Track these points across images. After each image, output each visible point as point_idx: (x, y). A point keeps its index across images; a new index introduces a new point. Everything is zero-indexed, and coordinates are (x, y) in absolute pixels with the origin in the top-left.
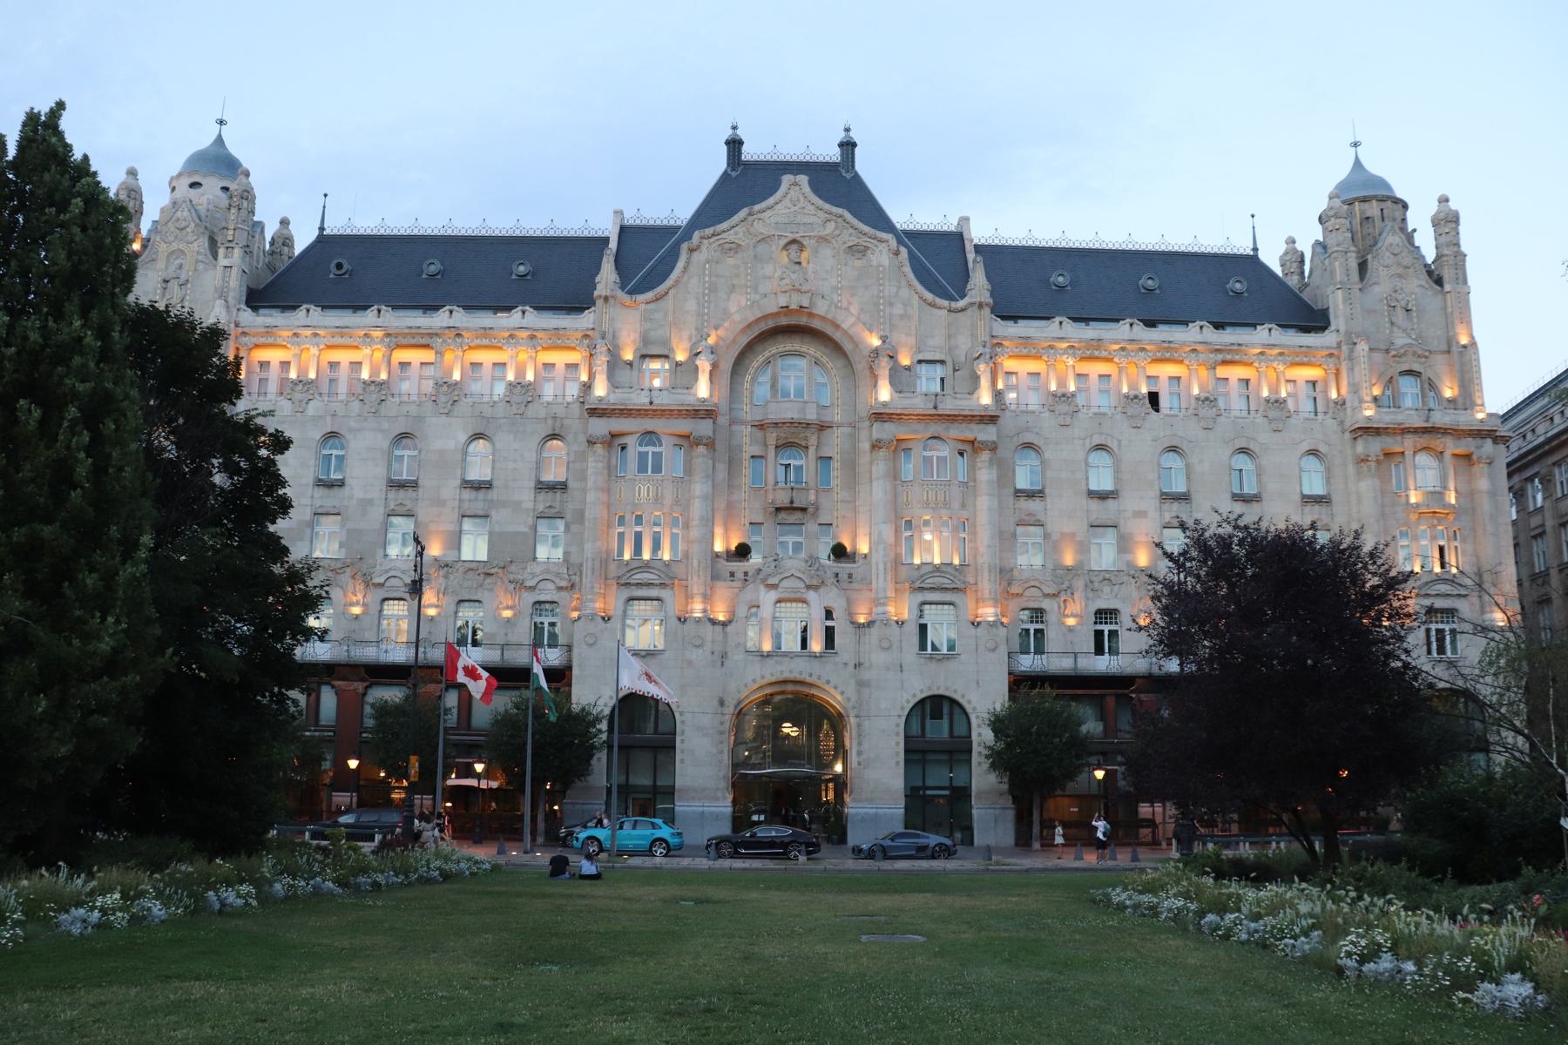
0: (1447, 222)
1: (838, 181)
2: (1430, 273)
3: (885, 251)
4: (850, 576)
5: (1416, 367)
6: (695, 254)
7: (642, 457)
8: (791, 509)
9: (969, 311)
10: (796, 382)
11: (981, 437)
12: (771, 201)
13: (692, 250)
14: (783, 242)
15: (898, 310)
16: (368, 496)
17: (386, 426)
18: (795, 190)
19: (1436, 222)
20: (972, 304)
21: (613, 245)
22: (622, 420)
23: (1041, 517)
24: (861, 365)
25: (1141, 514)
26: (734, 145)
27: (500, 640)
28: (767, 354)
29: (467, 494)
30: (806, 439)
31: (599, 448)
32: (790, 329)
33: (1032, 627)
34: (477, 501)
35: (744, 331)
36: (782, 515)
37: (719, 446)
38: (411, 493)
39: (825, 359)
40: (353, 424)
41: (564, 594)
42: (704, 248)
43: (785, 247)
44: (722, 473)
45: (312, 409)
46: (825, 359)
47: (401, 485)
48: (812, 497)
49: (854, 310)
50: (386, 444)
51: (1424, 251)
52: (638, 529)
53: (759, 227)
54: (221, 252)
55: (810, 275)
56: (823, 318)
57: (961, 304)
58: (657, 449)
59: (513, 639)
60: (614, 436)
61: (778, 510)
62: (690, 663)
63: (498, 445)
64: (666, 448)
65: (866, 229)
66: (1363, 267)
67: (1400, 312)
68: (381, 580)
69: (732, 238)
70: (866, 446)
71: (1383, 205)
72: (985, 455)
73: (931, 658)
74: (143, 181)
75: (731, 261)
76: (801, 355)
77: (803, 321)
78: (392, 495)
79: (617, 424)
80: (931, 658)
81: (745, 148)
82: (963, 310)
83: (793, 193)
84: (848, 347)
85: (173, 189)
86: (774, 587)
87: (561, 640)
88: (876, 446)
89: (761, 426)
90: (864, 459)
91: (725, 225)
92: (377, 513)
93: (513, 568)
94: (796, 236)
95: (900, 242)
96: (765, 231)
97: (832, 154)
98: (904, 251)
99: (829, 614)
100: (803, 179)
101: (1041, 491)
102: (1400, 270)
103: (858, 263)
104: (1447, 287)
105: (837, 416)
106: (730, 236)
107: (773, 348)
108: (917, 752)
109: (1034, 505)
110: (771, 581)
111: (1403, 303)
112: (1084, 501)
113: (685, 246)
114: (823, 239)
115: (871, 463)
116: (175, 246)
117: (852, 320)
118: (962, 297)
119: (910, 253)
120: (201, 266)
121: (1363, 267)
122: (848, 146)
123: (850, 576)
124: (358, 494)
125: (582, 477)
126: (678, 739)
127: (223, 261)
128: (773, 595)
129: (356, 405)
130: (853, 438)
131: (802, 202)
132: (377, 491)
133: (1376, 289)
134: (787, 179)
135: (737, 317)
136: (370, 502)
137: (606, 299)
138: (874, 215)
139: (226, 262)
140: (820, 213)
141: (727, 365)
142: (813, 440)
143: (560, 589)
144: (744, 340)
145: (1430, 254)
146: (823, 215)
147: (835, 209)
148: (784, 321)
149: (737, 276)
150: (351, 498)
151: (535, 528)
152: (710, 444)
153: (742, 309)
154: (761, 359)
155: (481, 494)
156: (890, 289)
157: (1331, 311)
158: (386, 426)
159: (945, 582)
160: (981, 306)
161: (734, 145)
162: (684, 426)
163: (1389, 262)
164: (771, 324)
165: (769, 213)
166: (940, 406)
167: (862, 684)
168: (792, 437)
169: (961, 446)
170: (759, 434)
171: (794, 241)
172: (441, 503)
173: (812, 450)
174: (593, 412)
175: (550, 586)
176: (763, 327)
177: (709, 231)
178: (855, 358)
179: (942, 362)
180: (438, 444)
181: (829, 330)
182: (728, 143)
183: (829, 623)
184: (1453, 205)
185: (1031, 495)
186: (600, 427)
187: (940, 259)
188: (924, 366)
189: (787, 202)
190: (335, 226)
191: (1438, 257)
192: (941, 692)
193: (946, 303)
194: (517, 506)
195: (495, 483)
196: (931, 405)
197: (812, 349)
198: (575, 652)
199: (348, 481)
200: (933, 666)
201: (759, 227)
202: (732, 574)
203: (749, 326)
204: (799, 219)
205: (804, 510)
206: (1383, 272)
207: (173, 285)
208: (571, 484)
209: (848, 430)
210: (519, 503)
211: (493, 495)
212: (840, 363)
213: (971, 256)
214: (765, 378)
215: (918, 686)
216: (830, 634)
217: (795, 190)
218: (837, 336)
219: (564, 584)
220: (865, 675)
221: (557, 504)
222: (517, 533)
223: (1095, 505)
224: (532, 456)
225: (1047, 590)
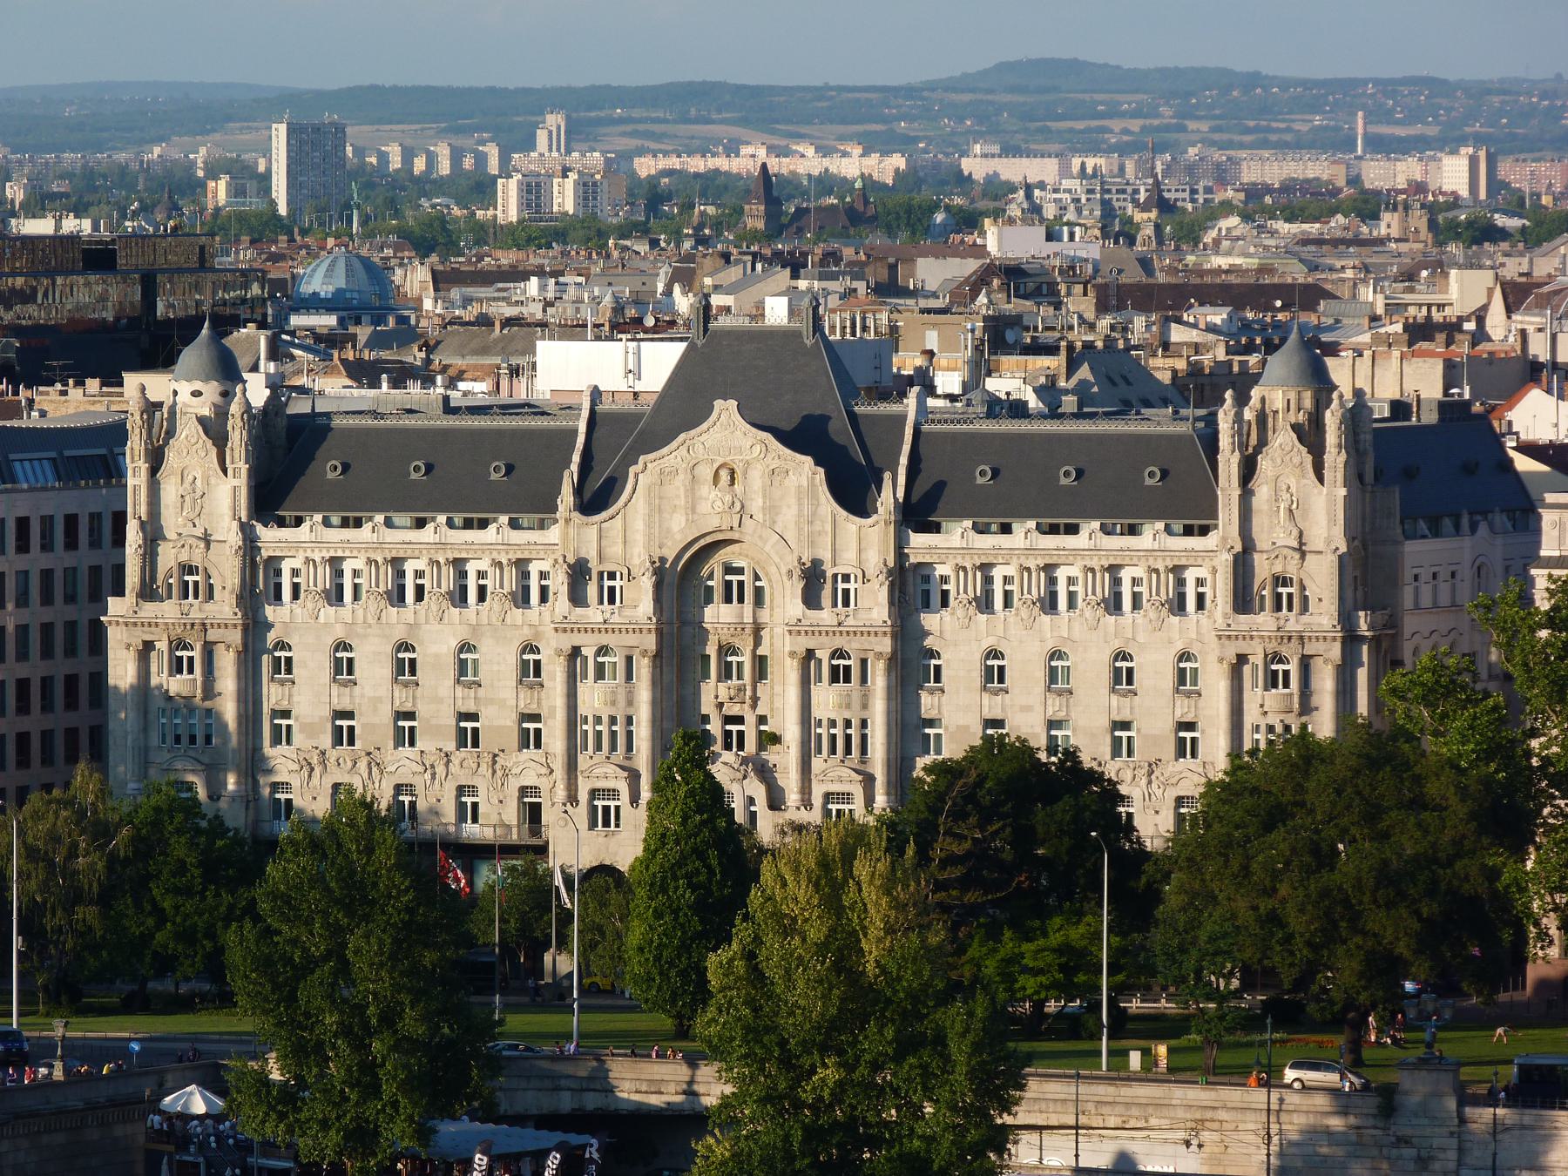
12: (705, 426)
14: (716, 466)
18: (726, 410)
25: (1027, 709)
41: (544, 779)
54: (230, 472)
91: (665, 450)
94: (728, 459)
98: (821, 470)
113: (632, 470)
134: (718, 403)
135: (678, 537)
136: (380, 699)
139: (236, 482)
149: (678, 496)
150: (362, 696)
162: (631, 640)
172: (440, 701)
180: (434, 649)
211: (481, 692)
217: (726, 410)
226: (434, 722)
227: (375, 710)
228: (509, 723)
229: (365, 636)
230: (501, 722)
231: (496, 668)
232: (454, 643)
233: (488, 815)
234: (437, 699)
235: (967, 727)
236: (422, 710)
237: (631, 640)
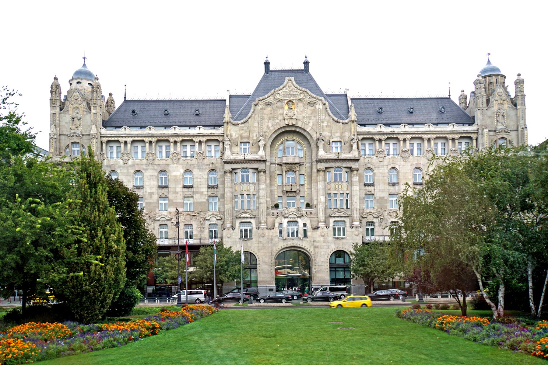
0: (519, 83)
1: (303, 74)
2: (512, 102)
3: (321, 103)
4: (311, 213)
5: (505, 136)
6: (257, 106)
8: (291, 192)
9: (349, 124)
10: (293, 151)
11: (353, 167)
13: (256, 105)
14: (286, 101)
15: (325, 124)
16: (152, 191)
17: (156, 167)
19: (516, 83)
20: (350, 121)
21: (227, 103)
22: (235, 164)
23: (373, 192)
24: (313, 144)
27: (199, 236)
28: (282, 140)
29: (186, 190)
30: (295, 168)
31: (228, 174)
32: (290, 131)
33: (370, 228)
34: (188, 192)
35: (274, 133)
36: (289, 194)
37: (267, 172)
38: (166, 190)
39: (301, 141)
40: (144, 167)
41: (219, 221)
42: (259, 104)
43: (287, 103)
44: (268, 181)
45: (130, 162)
46: (301, 141)
47: (163, 187)
48: (298, 188)
49: (311, 125)
50: (156, 174)
51: (510, 94)
52: (242, 200)
54: (92, 108)
55: (296, 113)
56: (300, 128)
58: (247, 174)
59: (203, 236)
60: (233, 169)
61: (287, 192)
62: (261, 242)
63: (194, 173)
64: (251, 173)
65: (314, 96)
66: (488, 101)
67: (501, 117)
68: (158, 219)
69: (269, 100)
70: (315, 171)
71: (497, 77)
72: (355, 172)
73: (337, 238)
74: (60, 81)
75: (269, 109)
76: (293, 140)
77: (293, 129)
78: (160, 191)
80: (337, 238)
81: (270, 65)
82: (347, 123)
83: (290, 84)
84: (308, 137)
85: (71, 84)
86: (287, 217)
87: (219, 236)
88: (318, 171)
89: (281, 165)
90: (315, 175)
91: (266, 96)
92: (156, 197)
93: (202, 213)
94: (291, 99)
95: (326, 100)
96: (280, 98)
98: (327, 103)
99: (305, 225)
100: (292, 78)
101: (373, 184)
102: (501, 102)
103: (312, 108)
104: (518, 107)
105: (306, 160)
106: (268, 100)
107: (283, 138)
108: (333, 269)
109: (371, 188)
110: (286, 216)
111: (502, 114)
112: (387, 187)
114: (300, 100)
115: (317, 176)
116: (75, 106)
117: (310, 128)
118: (347, 118)
119: (329, 104)
120: (85, 113)
121: (488, 101)
123: (311, 213)
124: (148, 190)
125: (223, 183)
126: (258, 266)
127: (93, 111)
128: (287, 220)
129: (145, 161)
130: (311, 168)
131: (293, 87)
132: (155, 190)
133: (493, 109)
134: (287, 78)
136: (153, 193)
137: (228, 123)
138: (318, 91)
139: (94, 112)
140: (299, 91)
141: (269, 145)
142: (298, 169)
143: (218, 220)
144: (274, 136)
145: (513, 95)
146: (300, 92)
147: (304, 89)
148: (287, 129)
150: (146, 192)
151: (208, 200)
152: (265, 172)
153: (271, 126)
154: (280, 142)
155: (190, 190)
156: (323, 117)
157: (476, 117)
158: (156, 167)
159: (342, 214)
160: (353, 122)
162: (255, 166)
163: (497, 99)
164: (283, 130)
165: (281, 91)
166: (340, 157)
167: (316, 247)
168: (291, 168)
169: (347, 170)
170: (280, 167)
171: (290, 101)
172: (177, 193)
173: (297, 172)
174: (226, 162)
175: (214, 219)
176: (280, 131)
178: (311, 141)
179: (340, 141)
180: (174, 174)
181: (302, 132)
182: (265, 63)
183: (305, 228)
184: (522, 77)
185: (369, 185)
186: (228, 167)
187: (339, 104)
188: (334, 143)
189: (287, 87)
191: (516, 96)
192: (341, 249)
193: (341, 121)
194: (202, 193)
195: (194, 186)
196: (336, 157)
197: (297, 138)
198: (224, 240)
199: (144, 186)
200: (338, 241)
201: (278, 96)
202: (273, 213)
203: (276, 131)
204: (292, 93)
205: (295, 192)
206: (495, 103)
207: (76, 120)
208: (219, 186)
209: (309, 165)
210: (203, 192)
211: (194, 190)
212: (306, 143)
213: (350, 103)
214: (281, 148)
215: (334, 248)
216: (305, 231)
218: (305, 134)
219: (219, 218)
220: (317, 244)
221: (215, 192)
222: (202, 202)
223: (391, 188)
224: (206, 177)
225: (375, 216)
226: (175, 201)
227: (151, 197)
228: (204, 201)
229: (147, 169)
230: (202, 201)
231: (199, 180)
232: (182, 171)
233: (197, 235)
235: (383, 197)
236: (171, 196)
237: (255, 166)
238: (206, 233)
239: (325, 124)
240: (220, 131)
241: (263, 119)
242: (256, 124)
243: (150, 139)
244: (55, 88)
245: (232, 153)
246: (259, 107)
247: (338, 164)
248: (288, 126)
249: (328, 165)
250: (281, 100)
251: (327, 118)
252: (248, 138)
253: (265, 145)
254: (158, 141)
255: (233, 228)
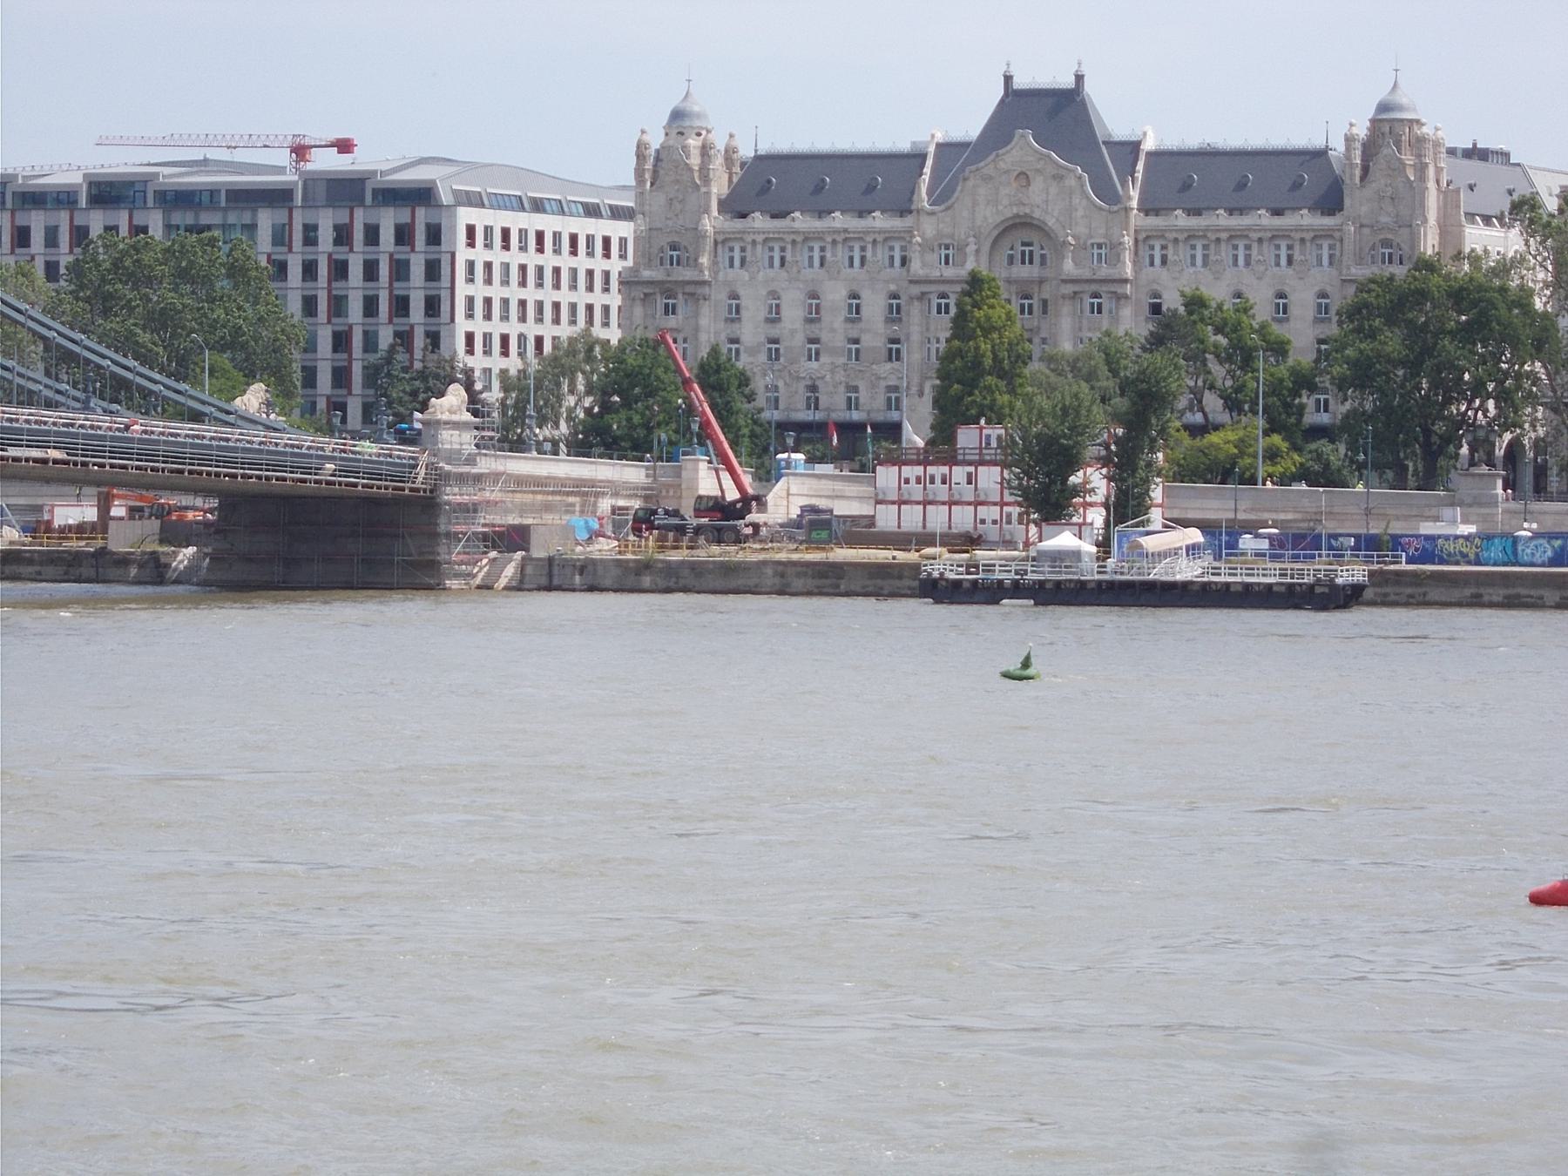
7: (939, 305)
11: (1120, 291)
15: (1080, 213)
26: (1008, 79)
29: (849, 325)
50: (802, 297)
53: (1002, 165)
57: (1115, 208)
60: (923, 294)
79: (925, 288)
97: (1068, 82)
106: (985, 171)
114: (1038, 170)
122: (1079, 78)
132: (799, 325)
141: (986, 248)
144: (996, 233)
161: (1008, 79)
171: (1022, 173)
172: (833, 330)
177: (973, 168)
190: (764, 148)
232: (844, 293)
234: (834, 328)
236: (824, 337)
238: (880, 401)
239: (1080, 213)
240: (908, 221)
241: (975, 204)
242: (965, 214)
243: (793, 237)
244: (641, 148)
245: (924, 265)
246: (970, 183)
247: (1094, 287)
248: (1017, 216)
249: (1077, 288)
250: (1007, 172)
251: (1084, 202)
252: (952, 236)
253: (977, 251)
254: (806, 239)
255: (921, 394)
